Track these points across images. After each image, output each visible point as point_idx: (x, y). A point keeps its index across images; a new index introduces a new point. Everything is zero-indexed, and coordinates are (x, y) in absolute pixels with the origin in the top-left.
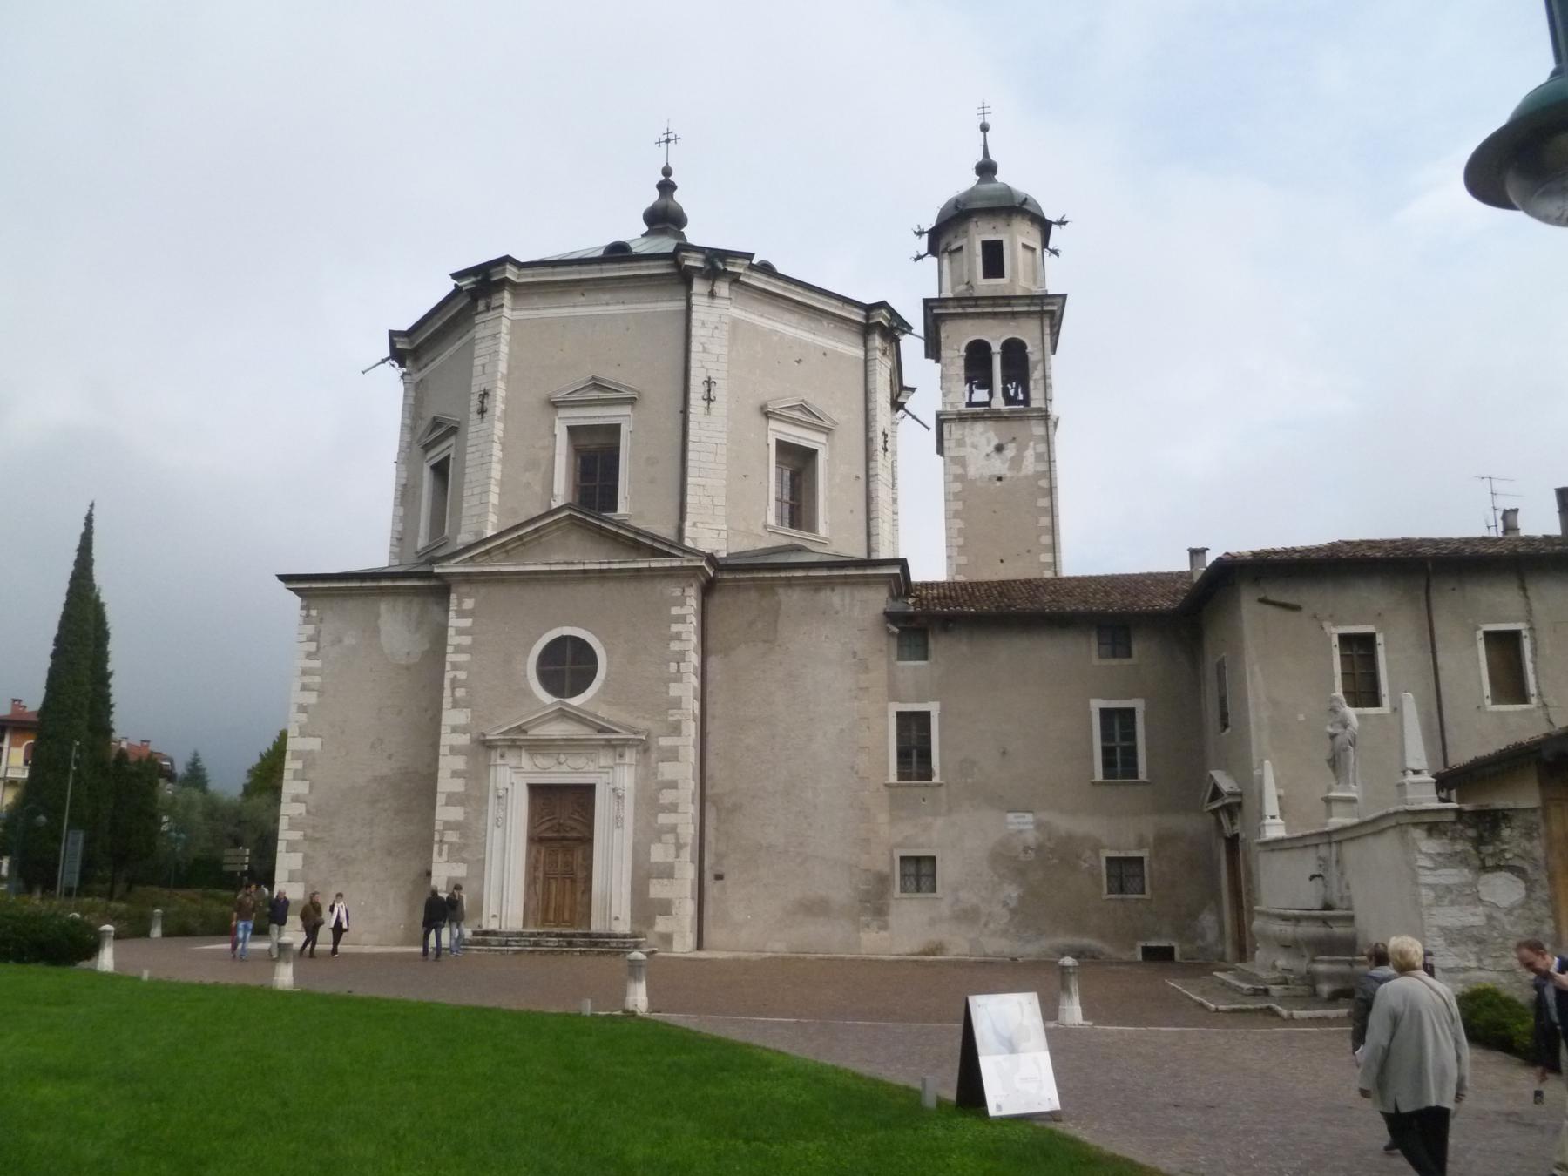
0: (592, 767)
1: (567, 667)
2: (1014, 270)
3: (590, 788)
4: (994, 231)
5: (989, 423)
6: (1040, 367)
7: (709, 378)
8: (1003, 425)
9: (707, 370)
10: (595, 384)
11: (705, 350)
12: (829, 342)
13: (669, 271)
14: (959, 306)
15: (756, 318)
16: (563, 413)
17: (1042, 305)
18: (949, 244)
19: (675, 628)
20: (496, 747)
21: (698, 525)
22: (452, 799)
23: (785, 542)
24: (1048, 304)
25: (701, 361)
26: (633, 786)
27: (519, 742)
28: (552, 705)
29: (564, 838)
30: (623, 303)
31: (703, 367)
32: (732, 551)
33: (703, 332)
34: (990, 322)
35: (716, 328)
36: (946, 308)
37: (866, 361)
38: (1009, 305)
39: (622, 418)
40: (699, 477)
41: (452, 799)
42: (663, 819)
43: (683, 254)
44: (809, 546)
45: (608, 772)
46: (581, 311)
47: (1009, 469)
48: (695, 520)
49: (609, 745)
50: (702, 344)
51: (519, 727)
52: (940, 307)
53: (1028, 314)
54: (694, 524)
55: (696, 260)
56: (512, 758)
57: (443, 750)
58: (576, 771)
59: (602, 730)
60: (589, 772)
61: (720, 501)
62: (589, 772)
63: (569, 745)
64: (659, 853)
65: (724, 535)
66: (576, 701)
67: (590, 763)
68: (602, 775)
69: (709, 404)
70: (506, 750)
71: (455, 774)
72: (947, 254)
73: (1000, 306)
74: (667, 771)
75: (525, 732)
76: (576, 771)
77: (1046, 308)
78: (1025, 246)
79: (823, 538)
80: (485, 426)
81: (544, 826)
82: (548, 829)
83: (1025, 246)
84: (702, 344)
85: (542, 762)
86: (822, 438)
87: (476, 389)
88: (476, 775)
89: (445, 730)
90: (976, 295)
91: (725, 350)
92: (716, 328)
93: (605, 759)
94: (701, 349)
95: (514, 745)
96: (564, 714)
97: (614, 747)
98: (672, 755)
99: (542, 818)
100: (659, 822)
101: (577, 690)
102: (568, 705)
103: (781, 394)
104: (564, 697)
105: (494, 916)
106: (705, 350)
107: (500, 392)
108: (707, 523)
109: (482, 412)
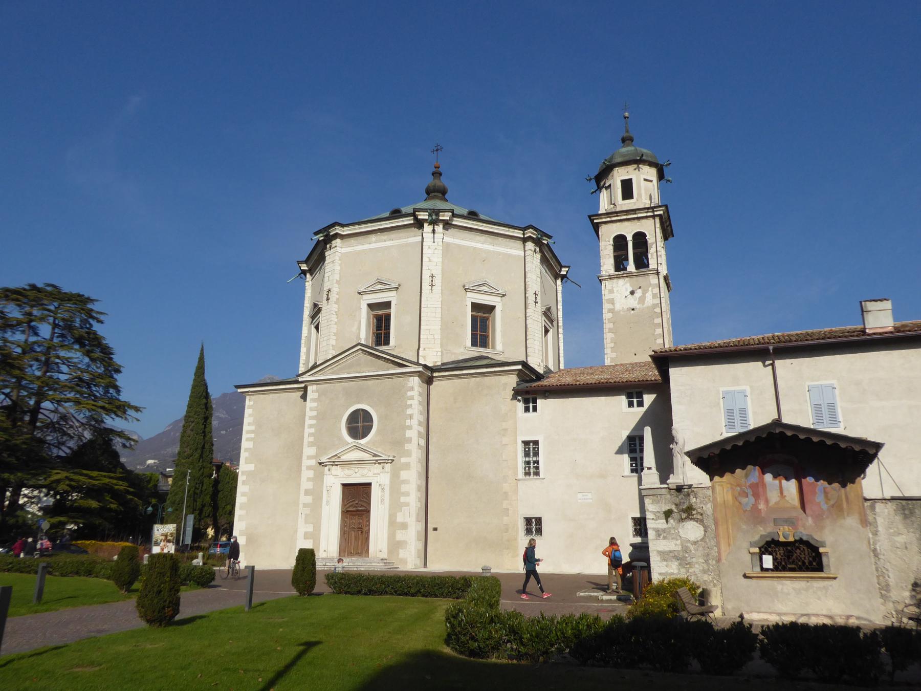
0: (371, 474)
1: (360, 424)
3: (370, 484)
5: (627, 279)
7: (432, 275)
9: (431, 270)
10: (379, 282)
11: (430, 261)
12: (503, 249)
13: (412, 222)
15: (460, 241)
16: (365, 297)
19: (409, 402)
20: (326, 466)
21: (426, 349)
22: (307, 492)
23: (476, 354)
25: (428, 266)
26: (389, 483)
27: (336, 462)
28: (352, 443)
29: (358, 511)
30: (392, 240)
31: (429, 269)
32: (445, 361)
33: (429, 251)
35: (436, 249)
37: (525, 256)
39: (392, 298)
40: (427, 325)
41: (307, 492)
42: (403, 499)
43: (417, 213)
44: (490, 356)
45: (377, 477)
46: (372, 246)
47: (638, 304)
48: (425, 347)
49: (377, 462)
50: (429, 258)
51: (336, 455)
54: (424, 349)
55: (424, 215)
56: (336, 470)
57: (304, 468)
58: (363, 476)
59: (375, 455)
60: (369, 477)
61: (438, 336)
62: (369, 477)
63: (361, 462)
64: (400, 519)
65: (439, 354)
66: (363, 441)
67: (369, 472)
68: (375, 478)
69: (432, 287)
70: (330, 467)
71: (309, 479)
74: (404, 475)
75: (339, 457)
76: (363, 476)
79: (498, 351)
80: (329, 306)
81: (348, 505)
82: (350, 506)
84: (429, 258)
85: (347, 471)
86: (498, 299)
87: (326, 289)
88: (318, 479)
89: (304, 457)
91: (440, 260)
92: (436, 249)
93: (377, 468)
94: (428, 260)
95: (334, 464)
96: (357, 448)
97: (380, 463)
98: (407, 466)
99: (348, 501)
100: (401, 501)
101: (364, 435)
102: (360, 444)
103: (472, 279)
104: (357, 439)
105: (325, 551)
106: (430, 261)
107: (335, 290)
108: (431, 348)
109: (328, 299)
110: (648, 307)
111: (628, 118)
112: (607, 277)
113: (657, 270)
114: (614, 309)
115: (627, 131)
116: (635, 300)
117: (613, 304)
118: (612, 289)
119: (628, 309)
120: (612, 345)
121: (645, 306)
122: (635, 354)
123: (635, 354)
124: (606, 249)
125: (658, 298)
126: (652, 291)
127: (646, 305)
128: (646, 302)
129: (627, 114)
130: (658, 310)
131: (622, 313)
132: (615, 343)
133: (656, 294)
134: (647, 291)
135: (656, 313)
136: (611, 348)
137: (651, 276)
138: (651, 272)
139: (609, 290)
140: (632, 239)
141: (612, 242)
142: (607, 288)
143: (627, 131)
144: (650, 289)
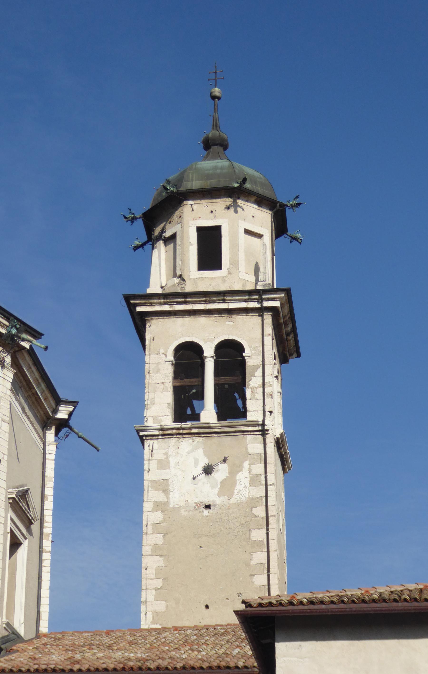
2: (234, 263)
4: (212, 215)
6: (259, 372)
8: (215, 440)
14: (165, 304)
17: (260, 300)
18: (163, 231)
24: (268, 300)
34: (203, 320)
36: (151, 304)
38: (224, 301)
52: (144, 304)
53: (246, 311)
72: (161, 242)
73: (213, 302)
77: (266, 304)
78: (247, 232)
83: (247, 232)
90: (189, 288)
110: (238, 504)
111: (219, 98)
112: (157, 433)
113: (263, 425)
114: (166, 504)
115: (215, 126)
116: (213, 487)
117: (166, 491)
118: (167, 458)
119: (197, 505)
120: (159, 583)
121: (233, 500)
122: (207, 607)
123: (207, 607)
124: (158, 371)
125: (261, 485)
126: (250, 470)
127: (235, 498)
128: (236, 492)
129: (217, 91)
130: (260, 511)
131: (183, 513)
132: (164, 579)
133: (258, 476)
134: (240, 468)
135: (256, 517)
136: (157, 589)
137: (250, 438)
138: (250, 428)
139: (160, 462)
140: (213, 354)
141: (171, 357)
142: (156, 456)
143: (215, 126)
144: (246, 464)
